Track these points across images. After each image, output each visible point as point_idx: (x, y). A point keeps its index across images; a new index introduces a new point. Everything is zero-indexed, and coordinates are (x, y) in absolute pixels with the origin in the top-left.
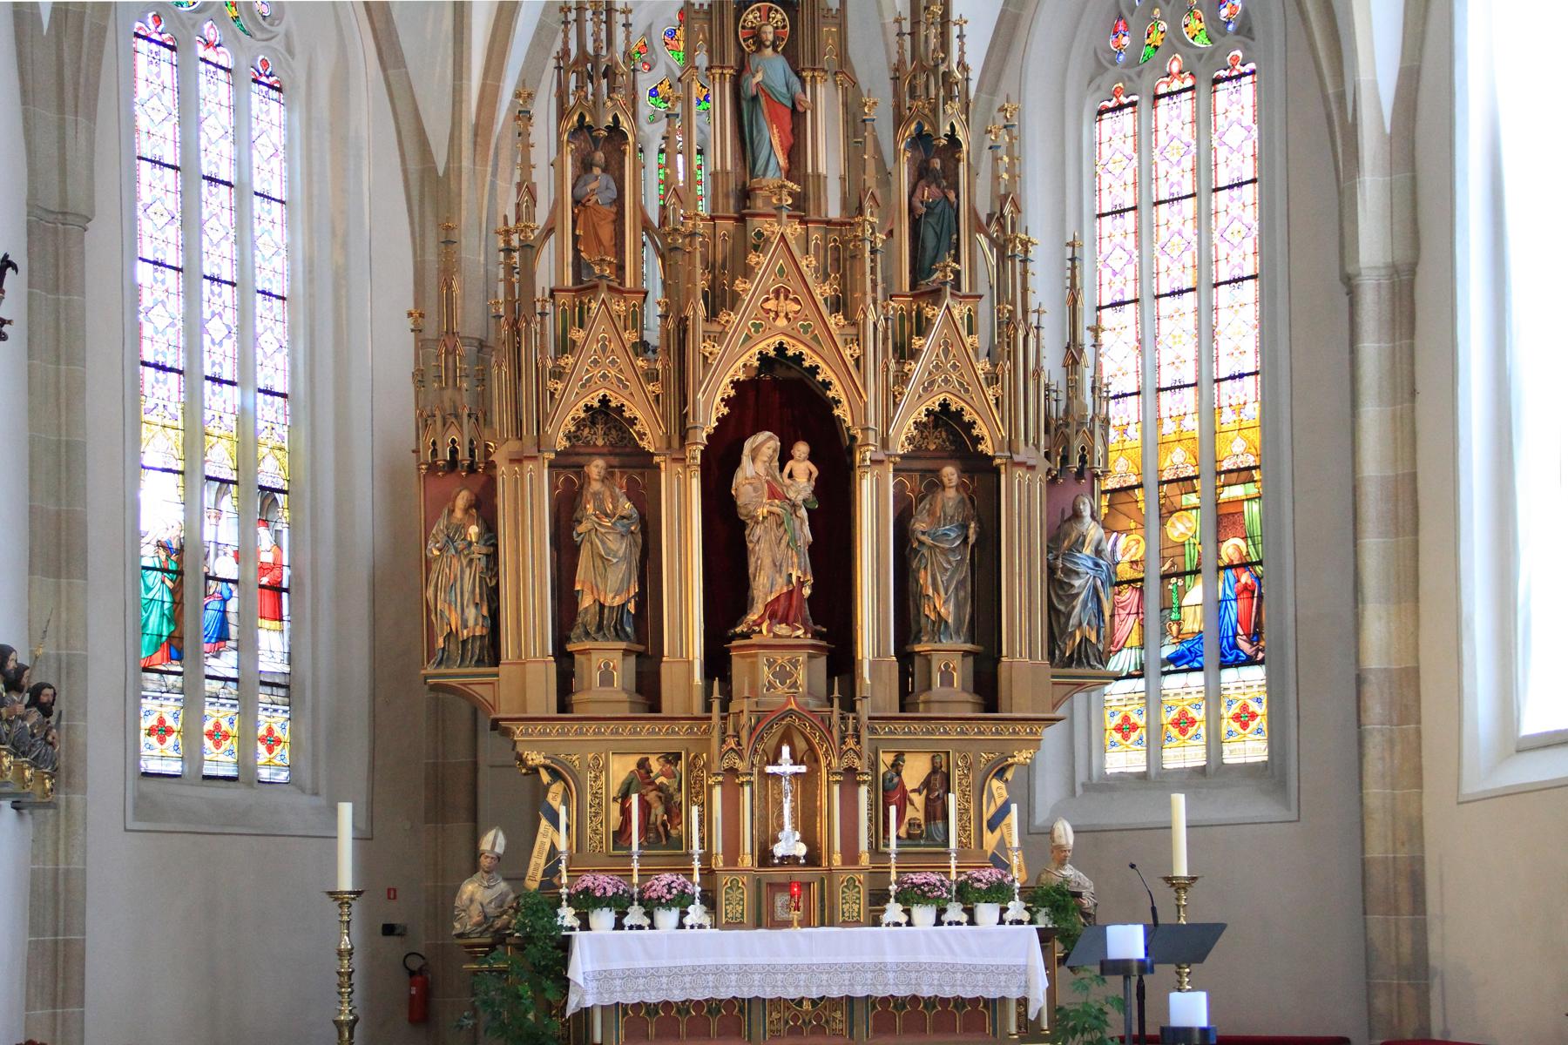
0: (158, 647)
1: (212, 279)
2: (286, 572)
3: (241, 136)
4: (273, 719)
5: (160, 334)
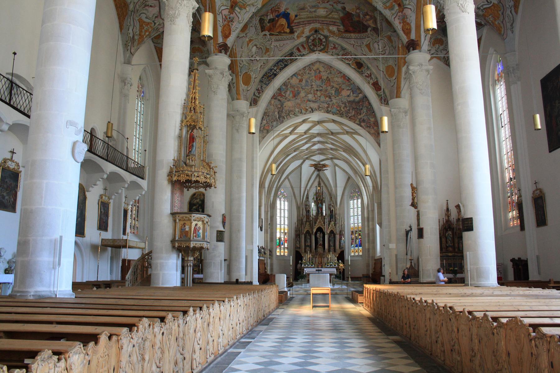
3: (284, 206)
4: (286, 251)
5: (278, 222)
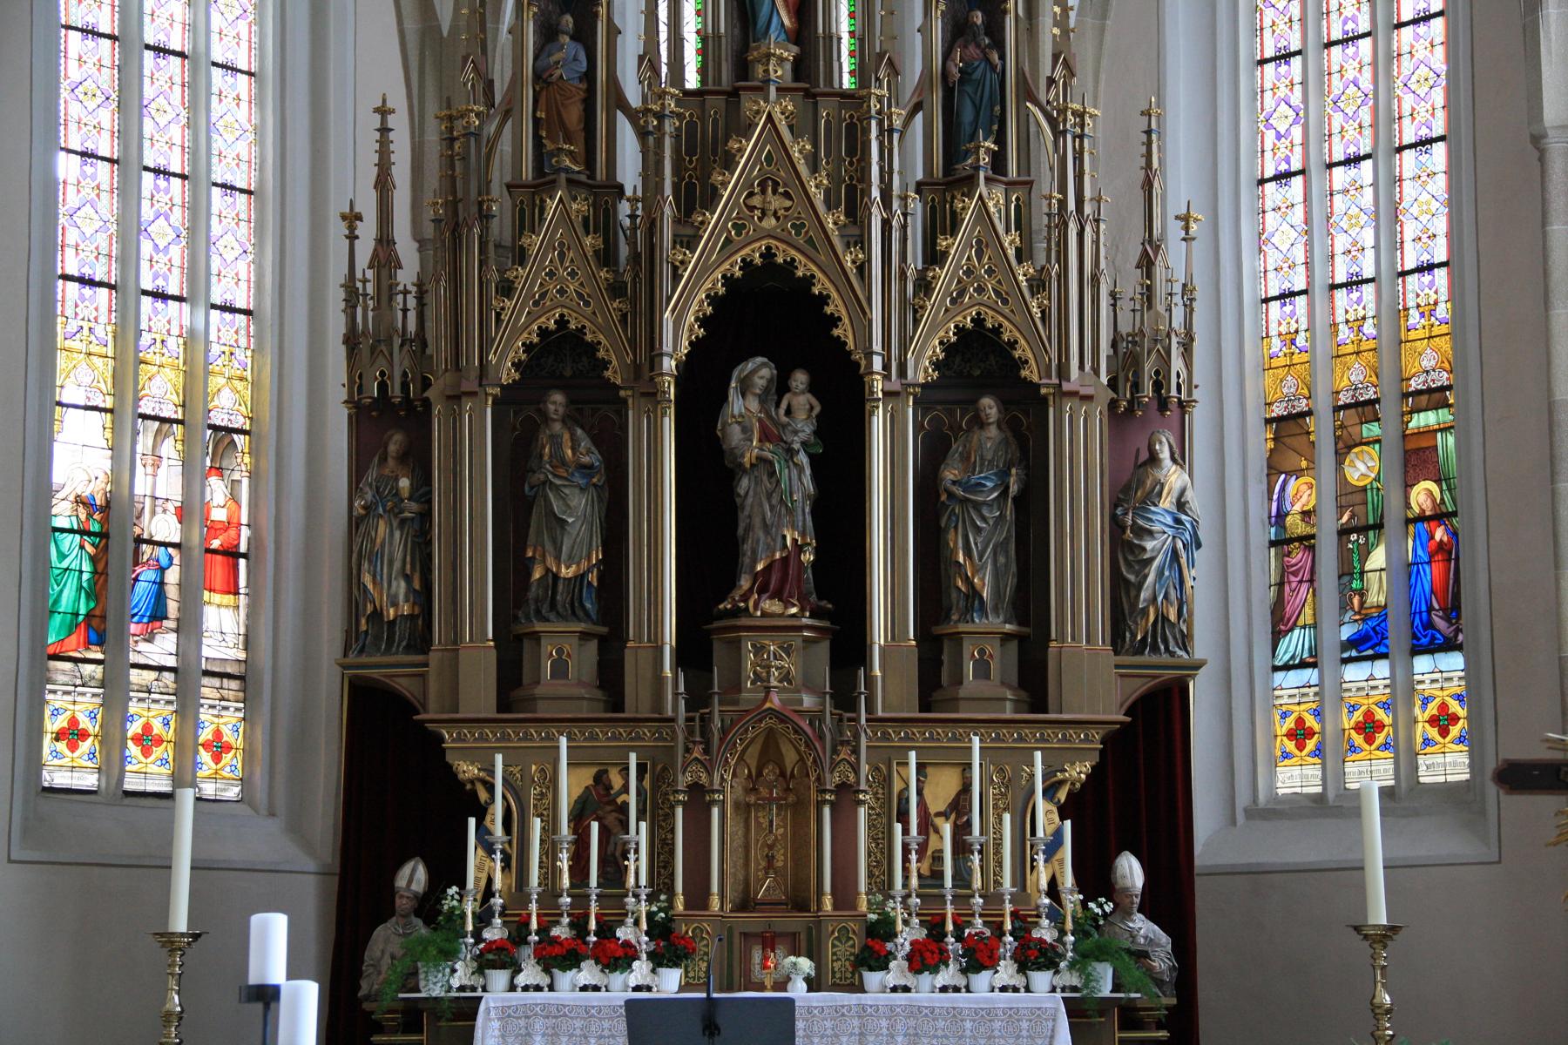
0: (73, 627)
1: (157, 171)
2: (245, 532)
4: (221, 717)
